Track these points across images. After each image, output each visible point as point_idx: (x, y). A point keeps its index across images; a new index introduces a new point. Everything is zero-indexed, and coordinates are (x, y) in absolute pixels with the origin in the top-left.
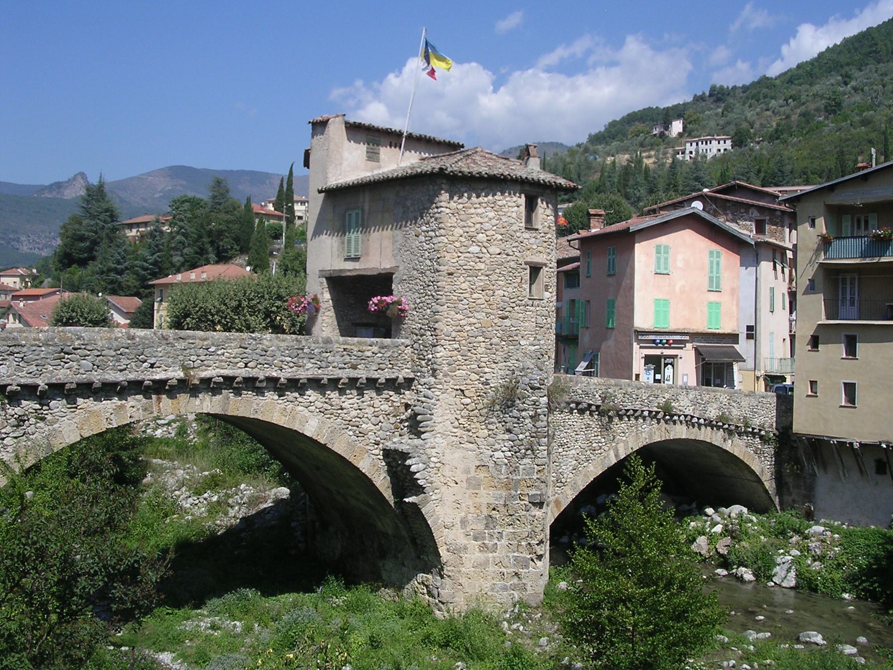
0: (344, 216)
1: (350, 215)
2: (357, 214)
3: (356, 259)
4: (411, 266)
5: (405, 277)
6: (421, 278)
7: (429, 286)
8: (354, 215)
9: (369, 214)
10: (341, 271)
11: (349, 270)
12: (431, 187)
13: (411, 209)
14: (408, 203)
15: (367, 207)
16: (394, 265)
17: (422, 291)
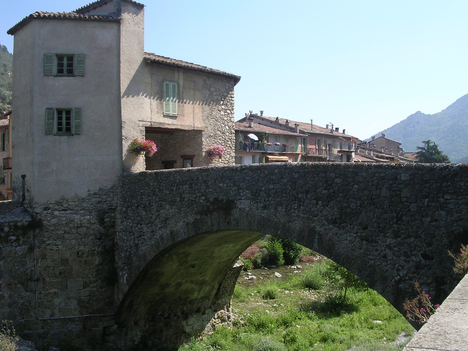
0: (162, 86)
1: (167, 85)
2: (174, 86)
3: (174, 117)
4: (216, 128)
5: (212, 134)
6: (223, 136)
7: (228, 141)
8: (171, 85)
9: (184, 88)
10: (161, 123)
11: (168, 124)
12: (228, 85)
13: (214, 93)
14: (213, 89)
15: (181, 82)
16: (204, 125)
17: (223, 144)
